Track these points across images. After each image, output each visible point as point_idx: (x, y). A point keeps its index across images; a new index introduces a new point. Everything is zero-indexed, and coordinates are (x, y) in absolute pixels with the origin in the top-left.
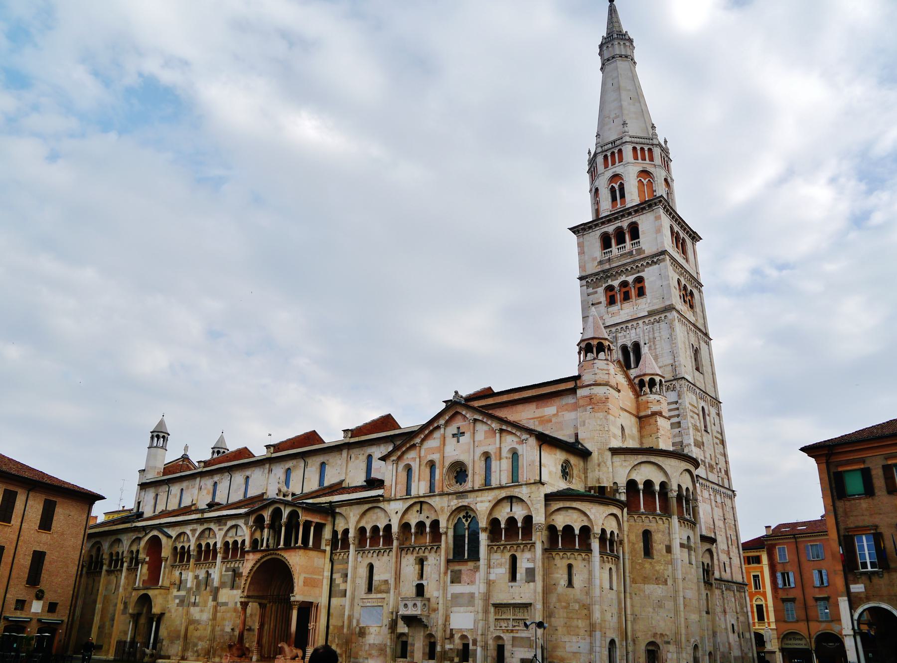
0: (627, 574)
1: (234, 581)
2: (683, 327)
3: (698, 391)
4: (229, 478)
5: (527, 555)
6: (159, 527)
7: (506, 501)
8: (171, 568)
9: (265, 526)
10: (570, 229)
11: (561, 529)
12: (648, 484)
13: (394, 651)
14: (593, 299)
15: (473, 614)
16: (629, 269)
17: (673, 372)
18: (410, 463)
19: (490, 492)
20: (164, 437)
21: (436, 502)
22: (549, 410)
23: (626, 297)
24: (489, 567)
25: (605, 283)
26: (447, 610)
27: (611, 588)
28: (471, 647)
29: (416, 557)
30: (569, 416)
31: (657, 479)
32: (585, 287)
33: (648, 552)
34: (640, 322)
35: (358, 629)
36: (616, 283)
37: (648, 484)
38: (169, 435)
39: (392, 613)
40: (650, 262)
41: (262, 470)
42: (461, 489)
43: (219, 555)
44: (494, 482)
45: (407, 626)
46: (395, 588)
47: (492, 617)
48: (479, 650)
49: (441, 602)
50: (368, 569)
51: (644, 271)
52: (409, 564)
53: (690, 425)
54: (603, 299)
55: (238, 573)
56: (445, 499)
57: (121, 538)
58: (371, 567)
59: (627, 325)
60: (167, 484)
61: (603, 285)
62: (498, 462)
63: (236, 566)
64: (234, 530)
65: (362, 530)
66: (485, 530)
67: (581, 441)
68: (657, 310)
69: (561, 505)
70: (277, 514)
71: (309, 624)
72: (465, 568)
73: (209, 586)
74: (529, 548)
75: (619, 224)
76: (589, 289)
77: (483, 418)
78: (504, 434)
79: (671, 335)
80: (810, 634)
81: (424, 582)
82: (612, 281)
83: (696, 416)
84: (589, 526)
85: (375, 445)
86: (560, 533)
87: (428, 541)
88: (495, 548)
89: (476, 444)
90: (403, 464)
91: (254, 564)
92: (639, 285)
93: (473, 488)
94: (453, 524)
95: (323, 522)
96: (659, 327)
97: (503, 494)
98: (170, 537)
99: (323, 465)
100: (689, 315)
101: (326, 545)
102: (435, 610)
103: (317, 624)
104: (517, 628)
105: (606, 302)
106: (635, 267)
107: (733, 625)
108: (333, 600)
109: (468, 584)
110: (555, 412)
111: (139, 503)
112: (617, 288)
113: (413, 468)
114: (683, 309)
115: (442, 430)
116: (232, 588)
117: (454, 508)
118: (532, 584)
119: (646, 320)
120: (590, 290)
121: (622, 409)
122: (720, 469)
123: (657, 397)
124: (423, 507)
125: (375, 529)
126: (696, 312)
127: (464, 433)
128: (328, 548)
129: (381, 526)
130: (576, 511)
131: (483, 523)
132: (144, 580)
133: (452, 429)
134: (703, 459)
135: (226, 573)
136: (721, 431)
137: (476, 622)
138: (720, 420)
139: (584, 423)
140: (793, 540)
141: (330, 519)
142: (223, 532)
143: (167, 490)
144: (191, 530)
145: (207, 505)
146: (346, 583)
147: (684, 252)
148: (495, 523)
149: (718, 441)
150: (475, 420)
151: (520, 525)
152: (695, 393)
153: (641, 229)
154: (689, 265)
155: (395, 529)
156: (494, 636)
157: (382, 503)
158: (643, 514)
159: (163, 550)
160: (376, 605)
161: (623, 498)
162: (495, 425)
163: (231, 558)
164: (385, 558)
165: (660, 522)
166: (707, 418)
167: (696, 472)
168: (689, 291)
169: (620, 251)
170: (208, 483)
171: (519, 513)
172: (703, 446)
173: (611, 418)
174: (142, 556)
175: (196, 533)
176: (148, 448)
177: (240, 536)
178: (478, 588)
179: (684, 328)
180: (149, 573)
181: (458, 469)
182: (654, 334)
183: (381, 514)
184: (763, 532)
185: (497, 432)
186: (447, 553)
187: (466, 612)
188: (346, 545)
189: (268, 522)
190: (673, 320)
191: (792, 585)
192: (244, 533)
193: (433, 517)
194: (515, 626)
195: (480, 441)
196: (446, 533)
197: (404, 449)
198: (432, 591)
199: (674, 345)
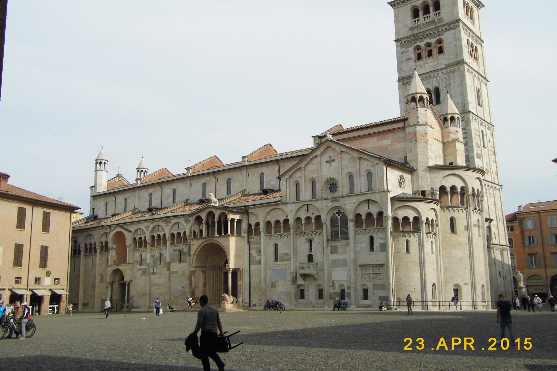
0: (441, 244)
1: (180, 257)
2: (470, 74)
3: (479, 119)
4: (161, 191)
5: (381, 235)
6: (121, 225)
7: (365, 202)
8: (133, 251)
9: (203, 223)
10: (388, 3)
11: (401, 219)
12: (453, 188)
13: (296, 295)
14: (405, 56)
16: (432, 33)
17: (463, 108)
18: (298, 180)
19: (354, 197)
20: (105, 163)
21: (318, 204)
22: (386, 141)
23: (430, 54)
24: (355, 243)
25: (414, 44)
26: (329, 270)
27: (433, 253)
28: (346, 291)
30: (399, 146)
31: (459, 184)
32: (400, 47)
33: (453, 230)
34: (440, 73)
35: (270, 284)
36: (422, 44)
37: (453, 188)
38: (108, 161)
39: (293, 273)
40: (448, 28)
41: (185, 185)
42: (334, 195)
43: (168, 242)
44: (357, 190)
45: (304, 280)
46: (294, 258)
48: (352, 292)
49: (325, 264)
50: (274, 246)
51: (443, 35)
52: (302, 243)
53: (474, 144)
55: (183, 253)
56: (324, 202)
57: (92, 234)
58: (276, 245)
59: (431, 75)
60: (113, 195)
61: (413, 46)
62: (358, 178)
63: (181, 248)
64: (177, 226)
65: (268, 223)
66: (352, 221)
67: (409, 162)
68: (452, 63)
69: (401, 204)
70: (211, 214)
71: (238, 282)
72: (340, 244)
73: (163, 261)
74: (381, 231)
76: (402, 49)
77: (347, 151)
78: (362, 160)
79: (462, 82)
80: (546, 276)
82: (419, 42)
83: (478, 137)
84: (419, 216)
85: (265, 166)
86: (401, 222)
87: (314, 229)
88: (359, 231)
89: (343, 167)
90: (293, 181)
91: (198, 247)
93: (342, 195)
94: (330, 217)
95: (241, 219)
96: (454, 76)
97: (363, 198)
98: (130, 232)
99: (229, 180)
100: (473, 64)
101: (244, 233)
102: (322, 270)
103: (243, 281)
105: (414, 58)
106: (436, 32)
107: (500, 272)
108: (251, 266)
109: (342, 253)
110: (390, 143)
111: (94, 209)
113: (300, 183)
114: (470, 62)
115: (319, 159)
116: (180, 262)
117: (330, 208)
118: (384, 253)
119: (444, 71)
120: (404, 49)
121: (435, 139)
122: (493, 171)
123: (456, 129)
124: (309, 208)
125: (277, 222)
126: (479, 62)
127: (334, 160)
128: (246, 235)
129: (281, 220)
130: (410, 208)
131: (351, 216)
132: (114, 260)
133: (326, 158)
134: (482, 166)
136: (494, 146)
137: (349, 275)
138: (493, 138)
139: (410, 150)
140: (538, 215)
141: (245, 216)
142: (169, 227)
143: (114, 199)
144: (145, 227)
145: (148, 209)
146: (260, 256)
147: (472, 18)
148: (358, 216)
149: (492, 153)
150: (342, 151)
151: (375, 217)
152: (477, 121)
154: (475, 27)
155: (291, 221)
156: (361, 284)
157: (281, 206)
158: (450, 207)
159: (126, 241)
160: (281, 268)
161: (438, 197)
162: (356, 155)
163: (177, 243)
164: (285, 239)
165: (461, 211)
166: (485, 137)
167: (482, 178)
168: (475, 47)
169: (425, 19)
170: (145, 194)
171: (374, 210)
172: (482, 157)
173: (429, 146)
174: (110, 245)
175: (149, 228)
176: (95, 171)
177: (182, 229)
178: (350, 255)
179: (471, 76)
180: (117, 255)
181: (331, 183)
182: (449, 80)
183: (280, 212)
184: (516, 210)
185: (357, 159)
186: (327, 236)
188: (258, 232)
189: (205, 220)
190: (464, 71)
191: (536, 244)
192: (187, 227)
193: (317, 214)
194: (374, 278)
195: (345, 165)
196: (326, 223)
197: (293, 171)
198: (317, 258)
199: (464, 89)
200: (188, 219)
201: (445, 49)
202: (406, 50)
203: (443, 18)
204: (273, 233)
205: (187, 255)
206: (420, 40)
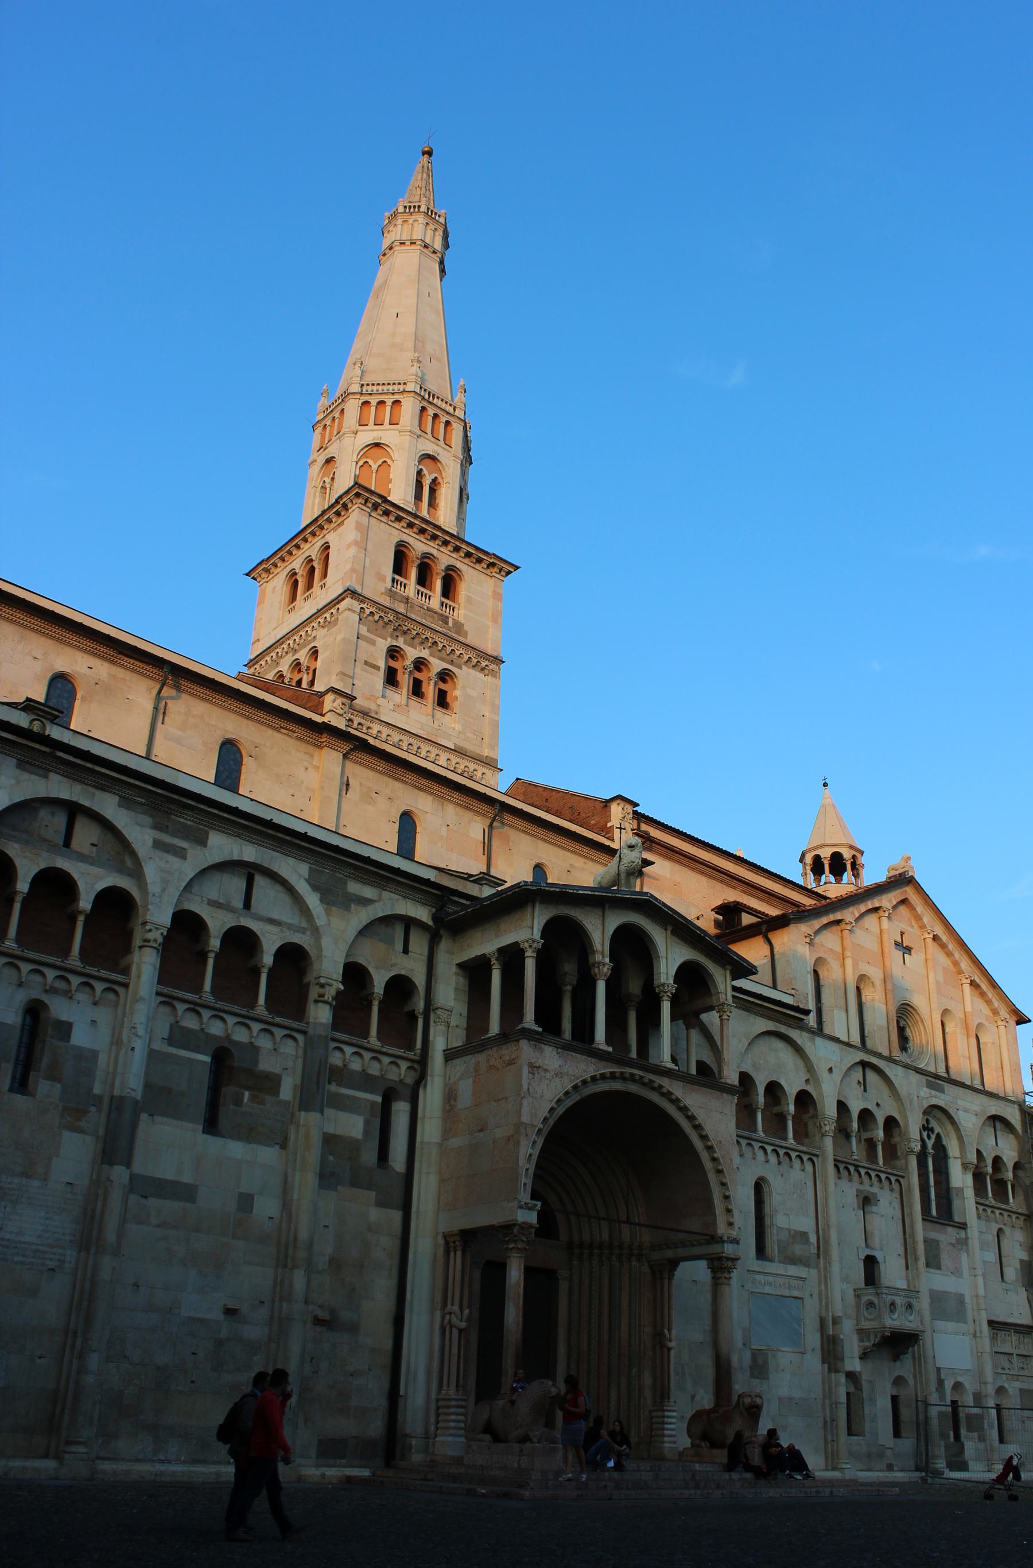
15: (967, 1338)
16: (440, 645)
25: (392, 637)
29: (857, 1190)
35: (747, 1356)
36: (412, 653)
47: (986, 1344)
51: (461, 668)
54: (382, 664)
59: (422, 746)
64: (236, 885)
73: (54, 1076)
75: (435, 552)
81: (879, 1256)
92: (442, 686)
104: (1022, 1373)
112: (409, 662)
135: (173, 1050)
137: (979, 1355)
153: (464, 590)
157: (798, 1032)
160: (787, 1293)
177: (271, 921)
187: (956, 1334)
193: (888, 1108)
200: (346, 883)
201: (456, 706)
202: (369, 635)
203: (466, 628)
204: (761, 1134)
205: (287, 1091)
206: (408, 637)
